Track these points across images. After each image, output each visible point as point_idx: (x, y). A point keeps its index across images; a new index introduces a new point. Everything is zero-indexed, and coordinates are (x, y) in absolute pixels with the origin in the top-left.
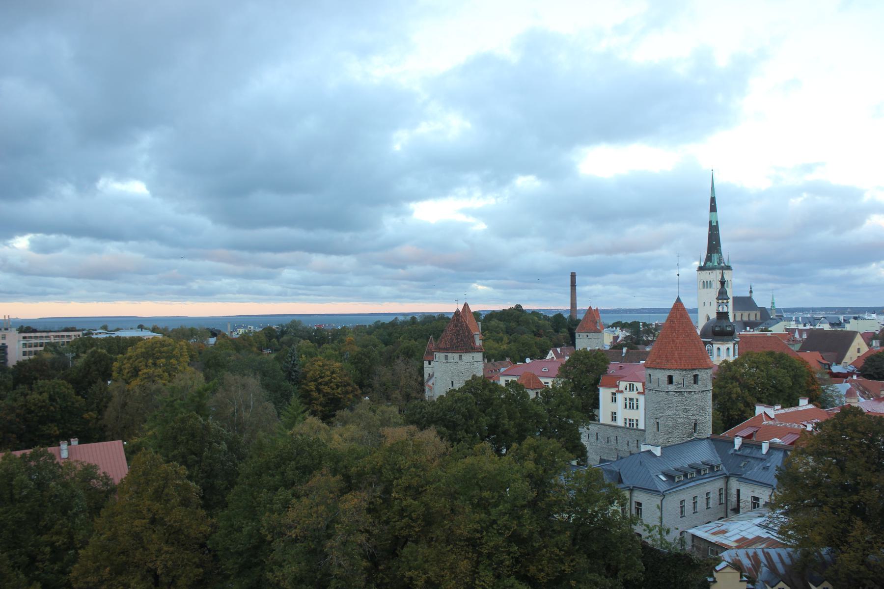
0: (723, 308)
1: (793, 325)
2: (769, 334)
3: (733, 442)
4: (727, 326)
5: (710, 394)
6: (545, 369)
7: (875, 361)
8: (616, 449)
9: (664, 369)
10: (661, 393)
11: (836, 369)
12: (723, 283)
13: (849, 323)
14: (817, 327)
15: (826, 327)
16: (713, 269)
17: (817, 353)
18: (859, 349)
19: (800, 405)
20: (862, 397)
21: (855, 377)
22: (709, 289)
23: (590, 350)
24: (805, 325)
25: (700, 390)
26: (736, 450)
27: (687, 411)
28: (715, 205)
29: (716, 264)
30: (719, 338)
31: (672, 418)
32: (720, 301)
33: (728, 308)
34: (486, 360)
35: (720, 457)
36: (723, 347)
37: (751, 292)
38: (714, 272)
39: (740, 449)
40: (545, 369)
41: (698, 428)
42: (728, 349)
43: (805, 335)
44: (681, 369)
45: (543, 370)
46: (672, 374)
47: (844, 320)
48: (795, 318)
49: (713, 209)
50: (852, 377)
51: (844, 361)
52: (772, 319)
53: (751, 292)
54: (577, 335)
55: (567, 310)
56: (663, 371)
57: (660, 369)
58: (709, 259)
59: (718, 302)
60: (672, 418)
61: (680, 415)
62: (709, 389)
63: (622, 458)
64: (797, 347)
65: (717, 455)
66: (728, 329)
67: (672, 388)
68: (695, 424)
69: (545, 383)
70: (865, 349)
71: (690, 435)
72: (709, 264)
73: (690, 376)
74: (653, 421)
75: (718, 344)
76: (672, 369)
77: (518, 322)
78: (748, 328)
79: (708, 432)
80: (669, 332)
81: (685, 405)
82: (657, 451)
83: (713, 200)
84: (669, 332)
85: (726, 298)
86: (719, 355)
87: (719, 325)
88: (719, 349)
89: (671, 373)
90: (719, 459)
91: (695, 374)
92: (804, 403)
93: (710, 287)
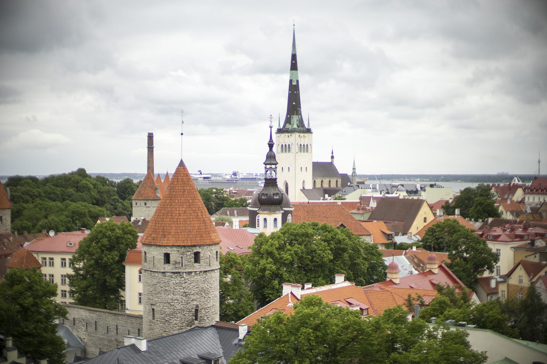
0: (271, 174)
1: (369, 193)
2: (339, 202)
3: (237, 330)
4: (274, 194)
5: (217, 274)
6: (71, 244)
7: (435, 232)
8: (116, 340)
9: (160, 246)
10: (156, 274)
11: (399, 239)
12: (271, 146)
13: (425, 190)
14: (394, 195)
15: (402, 195)
16: (293, 131)
17: (382, 223)
18: (425, 219)
19: (336, 282)
20: (416, 270)
21: (414, 249)
22: (288, 154)
23: (135, 221)
24: (381, 194)
25: (202, 269)
26: (240, 340)
27: (186, 294)
28: (296, 62)
29: (295, 126)
30: (265, 207)
31: (169, 303)
32: (268, 166)
33: (276, 174)
34: (16, 233)
35: (222, 348)
36: (270, 218)
37: (332, 157)
38: (293, 135)
39: (244, 337)
40: (71, 244)
41: (199, 315)
42: (275, 220)
43: (375, 203)
44: (179, 246)
45: (68, 245)
46: (169, 252)
47: (421, 188)
48: (373, 185)
49: (294, 67)
50: (412, 248)
51: (410, 231)
52: (349, 186)
53: (332, 157)
54: (134, 203)
55: (135, 175)
56: (159, 248)
57: (157, 246)
58: (288, 120)
59: (266, 168)
60: (169, 303)
61: (178, 300)
62: (213, 268)
63: (104, 353)
64: (366, 216)
65: (219, 346)
66: (275, 197)
67: (169, 268)
68: (197, 311)
69: (70, 259)
70: (431, 218)
71: (190, 323)
72: (288, 126)
73: (190, 255)
74: (149, 307)
75: (264, 214)
76: (169, 246)
77: (77, 187)
78: (327, 196)
79: (212, 319)
80: (168, 201)
81: (184, 288)
82: (143, 345)
83: (294, 57)
84: (168, 201)
85: (273, 162)
86: (265, 226)
87: (266, 193)
88: (265, 219)
89: (168, 250)
90: (221, 351)
91: (195, 251)
92: (340, 280)
93: (289, 151)
